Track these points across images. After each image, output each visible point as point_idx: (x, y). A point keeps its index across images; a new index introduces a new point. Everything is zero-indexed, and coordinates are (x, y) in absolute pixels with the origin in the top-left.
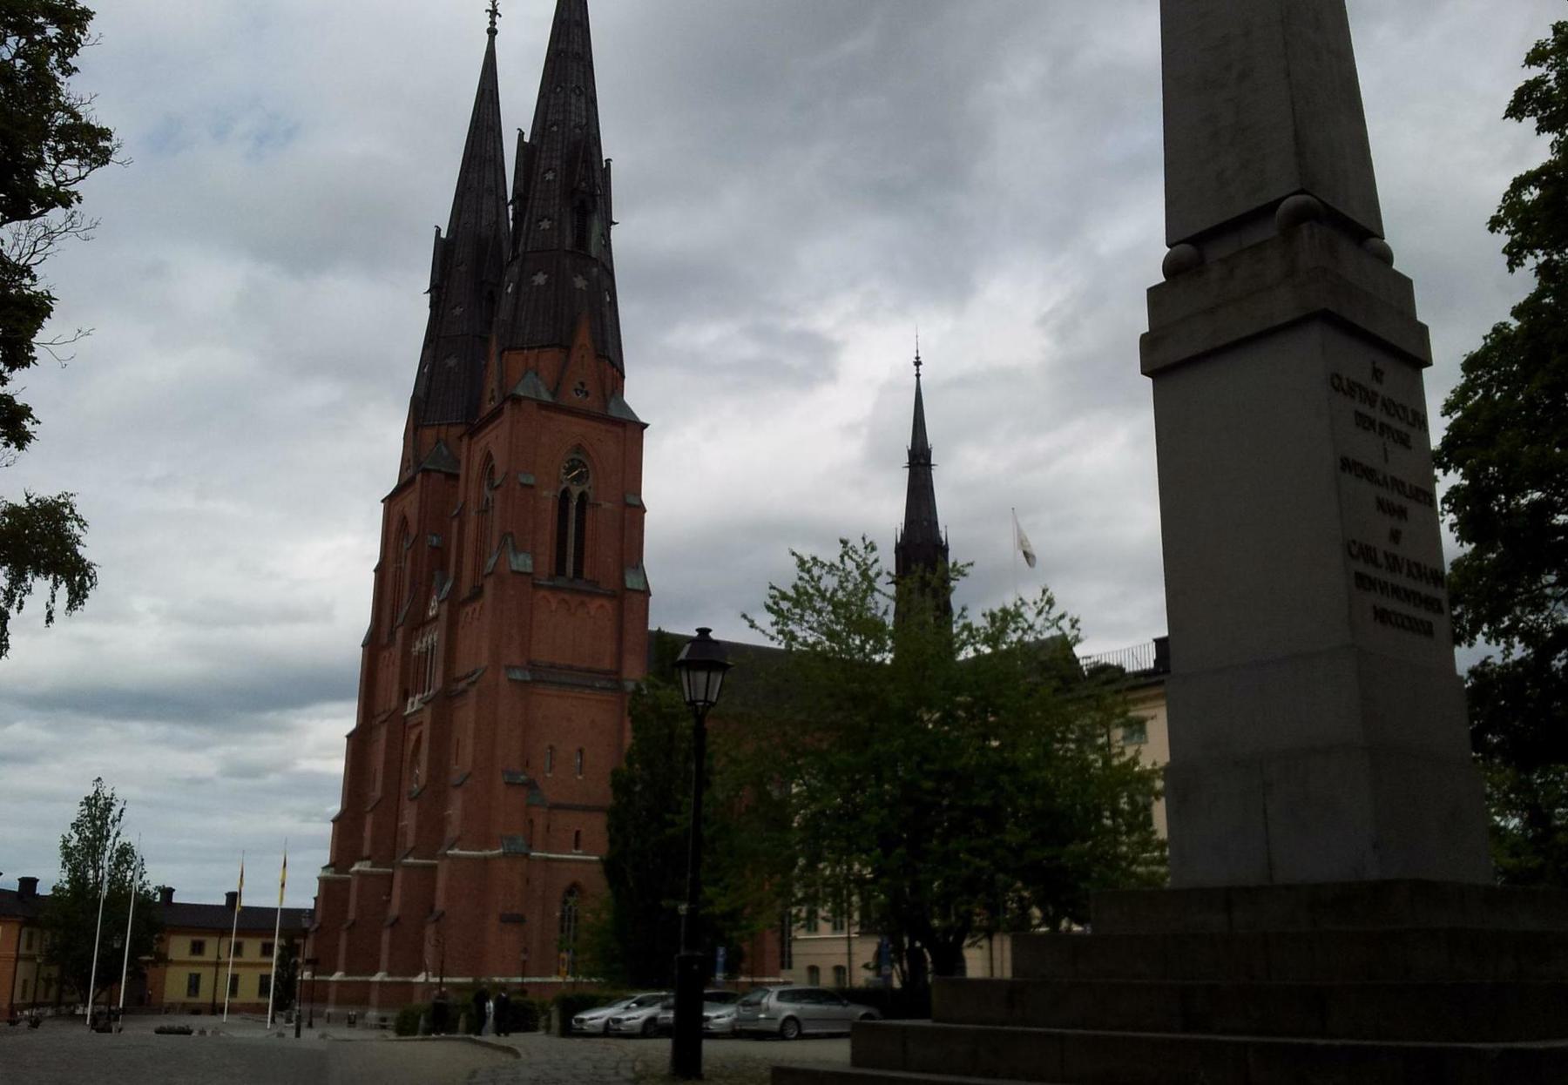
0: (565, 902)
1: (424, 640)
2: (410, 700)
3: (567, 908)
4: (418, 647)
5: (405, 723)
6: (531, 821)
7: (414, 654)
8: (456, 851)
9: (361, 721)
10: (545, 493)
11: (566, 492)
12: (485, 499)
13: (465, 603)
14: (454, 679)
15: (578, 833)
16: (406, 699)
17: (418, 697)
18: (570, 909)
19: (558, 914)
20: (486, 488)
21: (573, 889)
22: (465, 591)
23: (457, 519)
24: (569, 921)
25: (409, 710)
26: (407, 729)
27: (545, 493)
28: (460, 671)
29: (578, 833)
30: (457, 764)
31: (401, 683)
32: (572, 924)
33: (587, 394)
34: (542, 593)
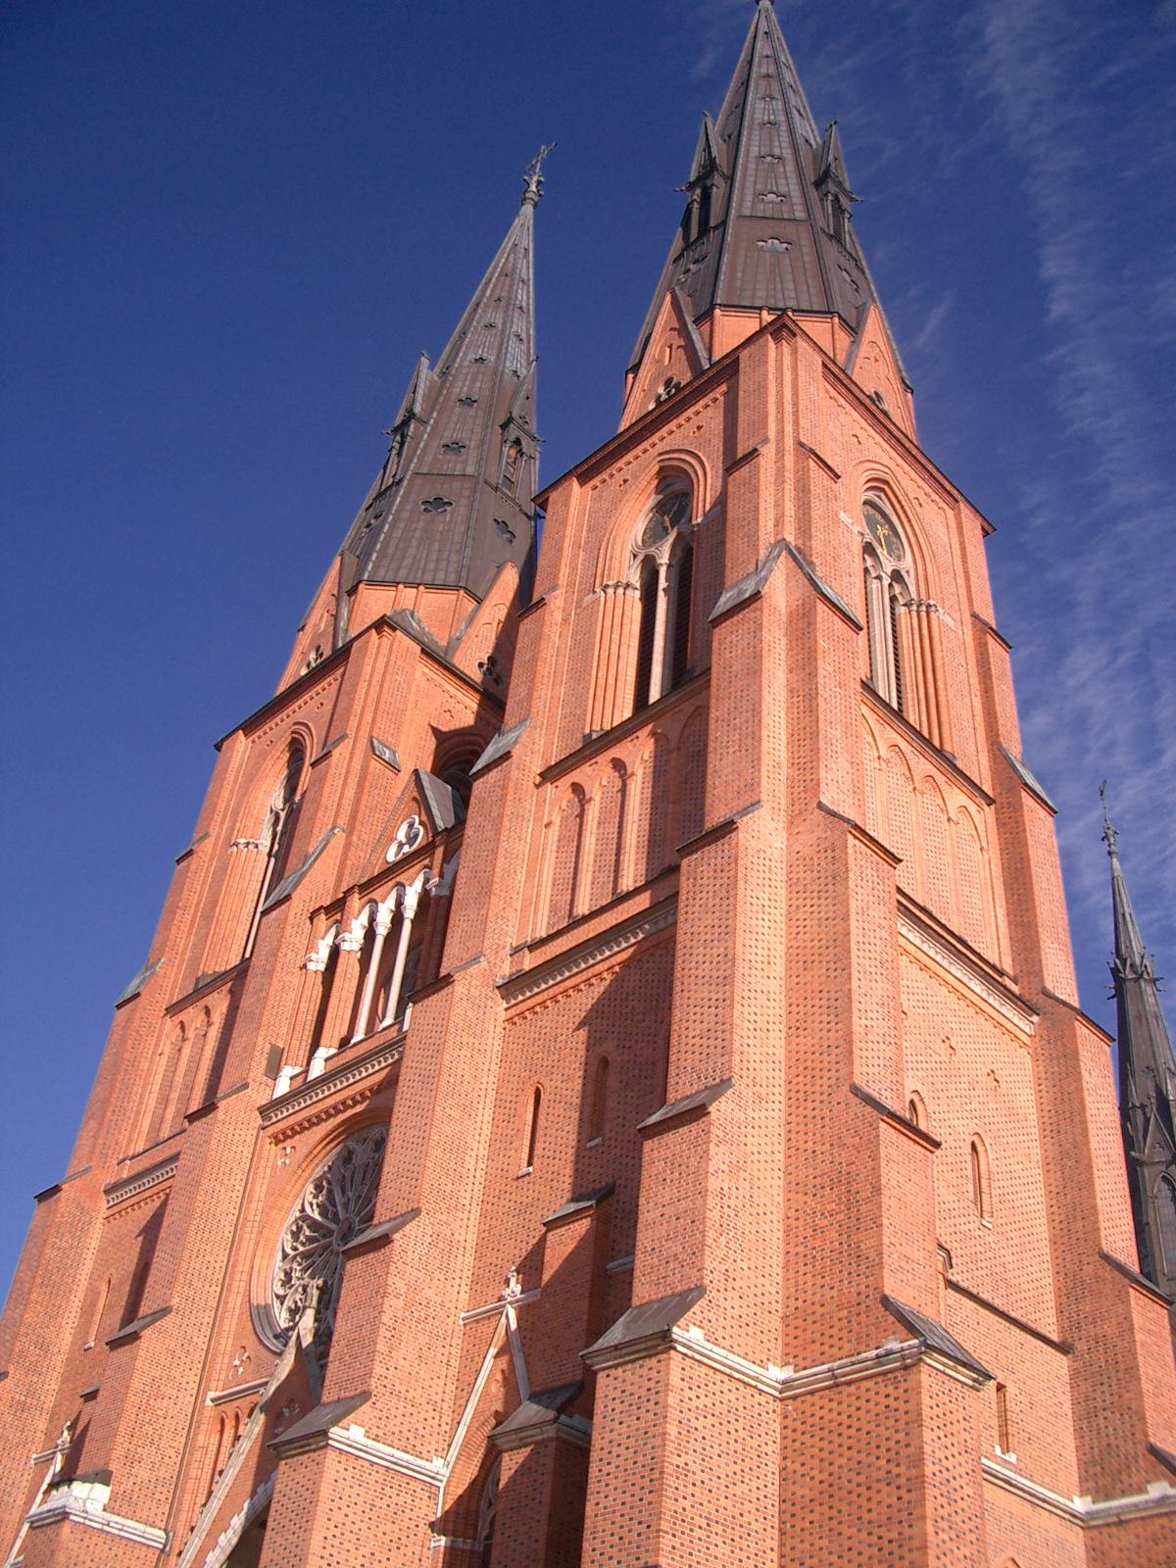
2: (288, 1071)
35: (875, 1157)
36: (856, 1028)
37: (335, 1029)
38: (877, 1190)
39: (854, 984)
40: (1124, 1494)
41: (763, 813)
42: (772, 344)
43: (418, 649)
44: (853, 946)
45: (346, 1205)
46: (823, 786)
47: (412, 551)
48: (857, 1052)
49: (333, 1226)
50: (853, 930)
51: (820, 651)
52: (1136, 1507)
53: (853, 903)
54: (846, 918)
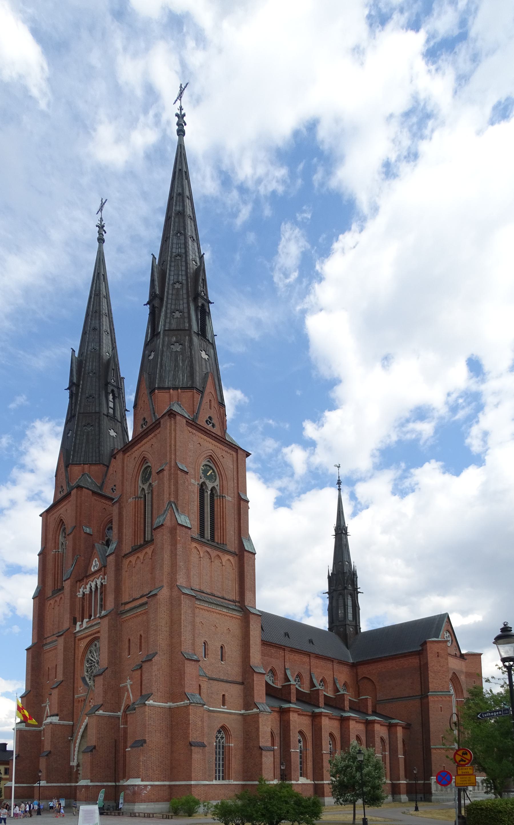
0: (217, 737)
1: (88, 586)
2: (78, 623)
3: (217, 740)
4: (83, 590)
5: (75, 637)
6: (200, 686)
7: (79, 596)
8: (151, 702)
9: (36, 641)
10: (193, 481)
11: (204, 483)
12: (140, 490)
13: (126, 556)
14: (122, 604)
15: (224, 695)
16: (75, 623)
17: (85, 620)
18: (219, 742)
19: (215, 744)
20: (140, 482)
21: (223, 728)
22: (127, 548)
23: (117, 504)
24: (219, 748)
25: (78, 629)
26: (77, 641)
27: (193, 481)
28: (126, 598)
29: (224, 695)
30: (129, 654)
31: (71, 613)
32: (221, 750)
33: (213, 426)
34: (194, 545)
35: (184, 667)
36: (182, 639)
37: (87, 614)
38: (184, 673)
39: (182, 630)
40: (250, 710)
41: (164, 588)
42: (169, 420)
43: (91, 493)
44: (182, 621)
45: (97, 656)
46: (178, 580)
47: (83, 449)
48: (182, 644)
49: (95, 661)
50: (182, 618)
51: (178, 541)
52: (251, 713)
53: (182, 611)
54: (181, 615)
